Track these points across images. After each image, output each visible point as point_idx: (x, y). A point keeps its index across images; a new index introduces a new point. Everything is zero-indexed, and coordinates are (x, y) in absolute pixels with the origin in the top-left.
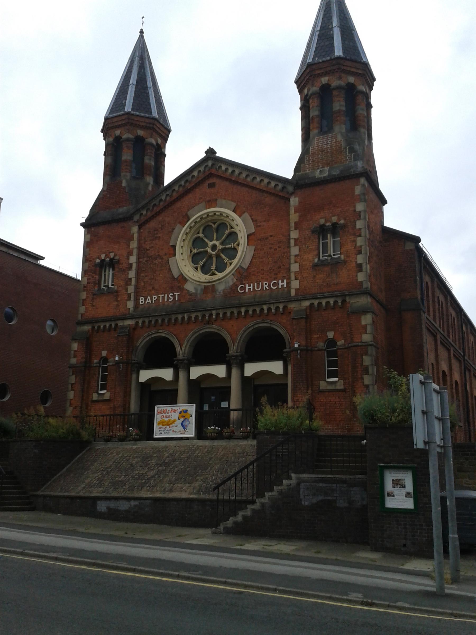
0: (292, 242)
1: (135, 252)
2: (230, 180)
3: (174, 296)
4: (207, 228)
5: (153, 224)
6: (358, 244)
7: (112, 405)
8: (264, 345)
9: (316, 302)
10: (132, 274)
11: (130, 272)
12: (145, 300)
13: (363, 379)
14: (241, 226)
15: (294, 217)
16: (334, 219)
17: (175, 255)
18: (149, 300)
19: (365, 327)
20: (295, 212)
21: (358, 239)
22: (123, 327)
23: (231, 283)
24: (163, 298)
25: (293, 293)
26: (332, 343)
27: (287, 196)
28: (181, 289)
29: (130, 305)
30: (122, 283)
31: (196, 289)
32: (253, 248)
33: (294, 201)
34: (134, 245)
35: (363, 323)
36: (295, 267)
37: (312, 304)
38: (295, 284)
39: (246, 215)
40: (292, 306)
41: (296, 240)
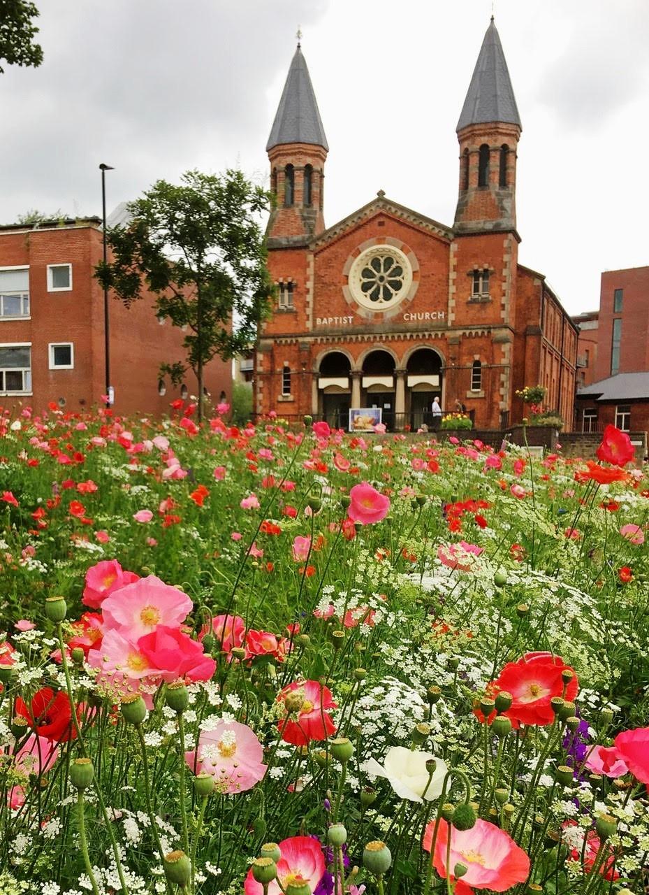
0: (451, 282)
1: (312, 278)
2: (398, 221)
3: (348, 320)
4: (375, 262)
5: (325, 254)
6: (503, 288)
7: (296, 405)
8: (424, 361)
9: (467, 332)
10: (310, 298)
11: (307, 296)
12: (322, 320)
13: (499, 390)
14: (408, 264)
15: (453, 261)
16: (486, 266)
17: (347, 284)
18: (325, 321)
19: (504, 353)
20: (455, 256)
21: (504, 284)
22: (304, 343)
23: (397, 312)
24: (338, 320)
25: (449, 324)
26: (477, 363)
27: (448, 242)
28: (353, 314)
29: (309, 324)
30: (301, 305)
31: (367, 315)
32: (418, 283)
33: (454, 247)
34: (310, 271)
35: (503, 350)
36: (452, 303)
37: (464, 333)
38: (452, 317)
39: (412, 253)
40: (448, 334)
41: (454, 280)
